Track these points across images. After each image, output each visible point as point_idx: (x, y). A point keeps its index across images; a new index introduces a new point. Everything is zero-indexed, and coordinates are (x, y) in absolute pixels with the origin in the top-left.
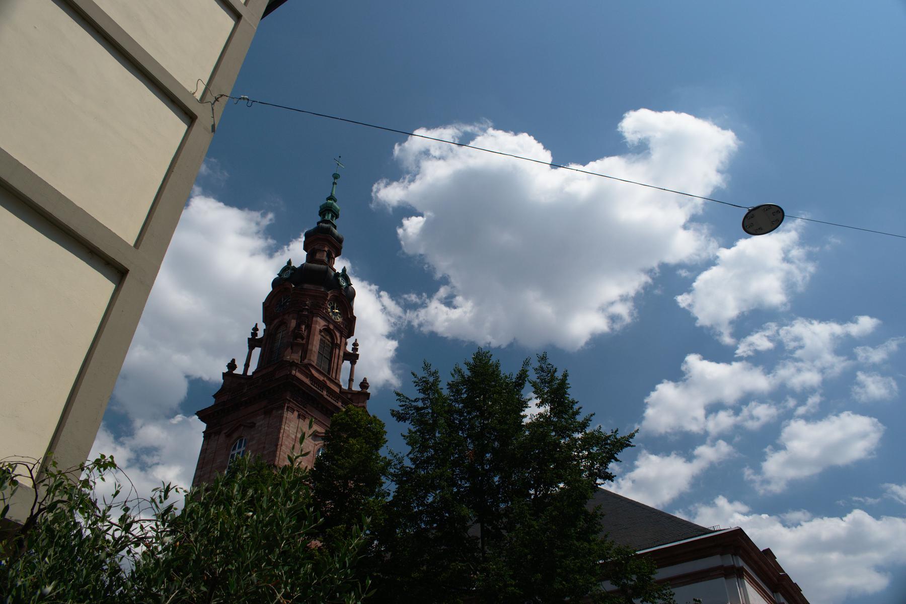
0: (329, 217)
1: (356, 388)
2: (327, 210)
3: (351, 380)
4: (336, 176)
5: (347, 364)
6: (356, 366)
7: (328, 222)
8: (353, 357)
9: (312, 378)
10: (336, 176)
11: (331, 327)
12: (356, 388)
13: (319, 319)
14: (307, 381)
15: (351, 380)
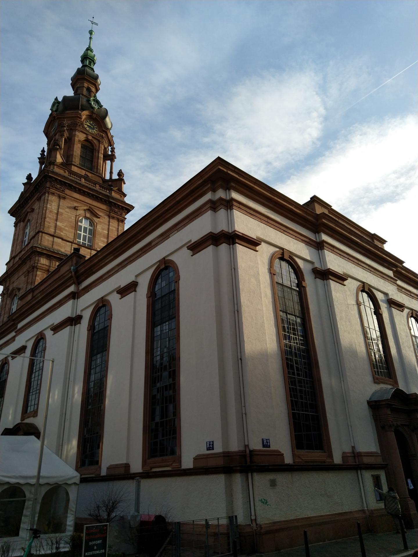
0: (87, 63)
1: (115, 177)
2: (87, 58)
3: (111, 173)
4: (91, 32)
5: (108, 162)
6: (114, 164)
7: (86, 66)
8: (112, 158)
9: (71, 173)
10: (91, 32)
11: (90, 138)
12: (115, 177)
13: (77, 133)
14: (66, 174)
15: (111, 173)
